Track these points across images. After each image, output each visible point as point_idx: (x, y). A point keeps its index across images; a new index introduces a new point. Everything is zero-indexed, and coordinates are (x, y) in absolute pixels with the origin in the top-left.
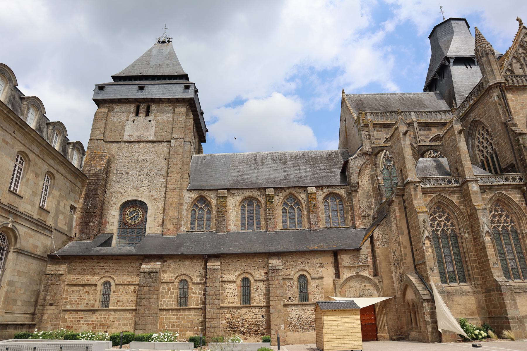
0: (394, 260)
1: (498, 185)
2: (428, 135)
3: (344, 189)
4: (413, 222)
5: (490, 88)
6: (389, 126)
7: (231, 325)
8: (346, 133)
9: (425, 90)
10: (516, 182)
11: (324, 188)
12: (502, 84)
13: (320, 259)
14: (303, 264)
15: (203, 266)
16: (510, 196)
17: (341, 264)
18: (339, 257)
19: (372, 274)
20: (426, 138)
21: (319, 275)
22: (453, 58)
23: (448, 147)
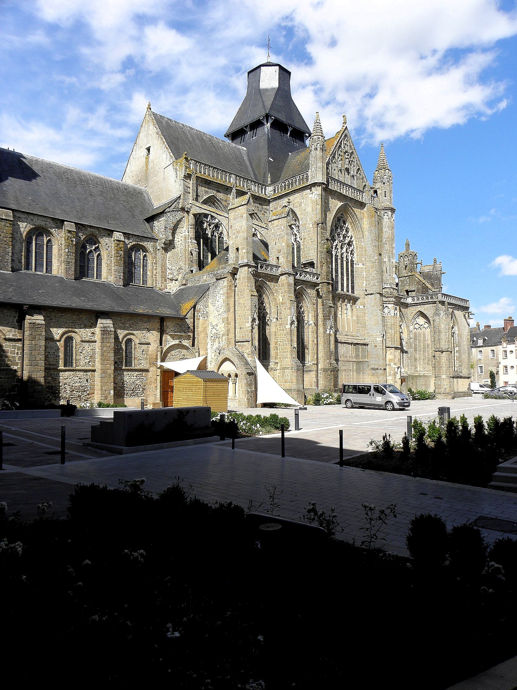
0: (213, 333)
4: (241, 301)
5: (314, 185)
6: (210, 183)
7: (52, 390)
8: (147, 166)
9: (227, 136)
13: (148, 324)
14: (131, 327)
15: (17, 318)
19: (191, 343)
21: (147, 341)
23: (273, 234)
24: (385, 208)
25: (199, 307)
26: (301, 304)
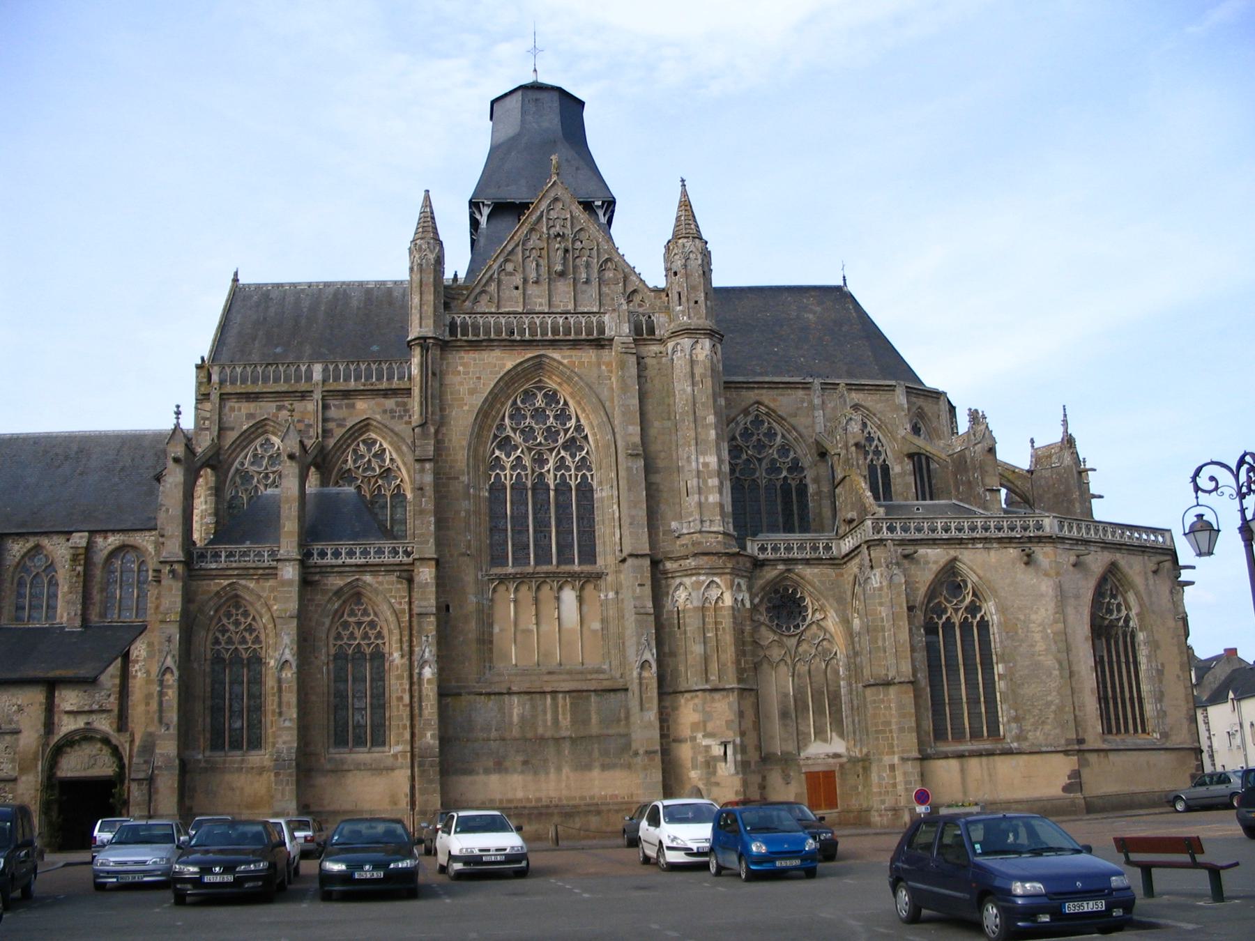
1: (357, 566)
2: (344, 419)
3: (153, 538)
10: (397, 560)
11: (109, 534)
12: (428, 341)
16: (381, 588)
17: (59, 706)
18: (57, 694)
19: (115, 726)
20: (340, 426)
22: (489, 206)
24: (672, 333)
25: (135, 655)
26: (372, 617)
